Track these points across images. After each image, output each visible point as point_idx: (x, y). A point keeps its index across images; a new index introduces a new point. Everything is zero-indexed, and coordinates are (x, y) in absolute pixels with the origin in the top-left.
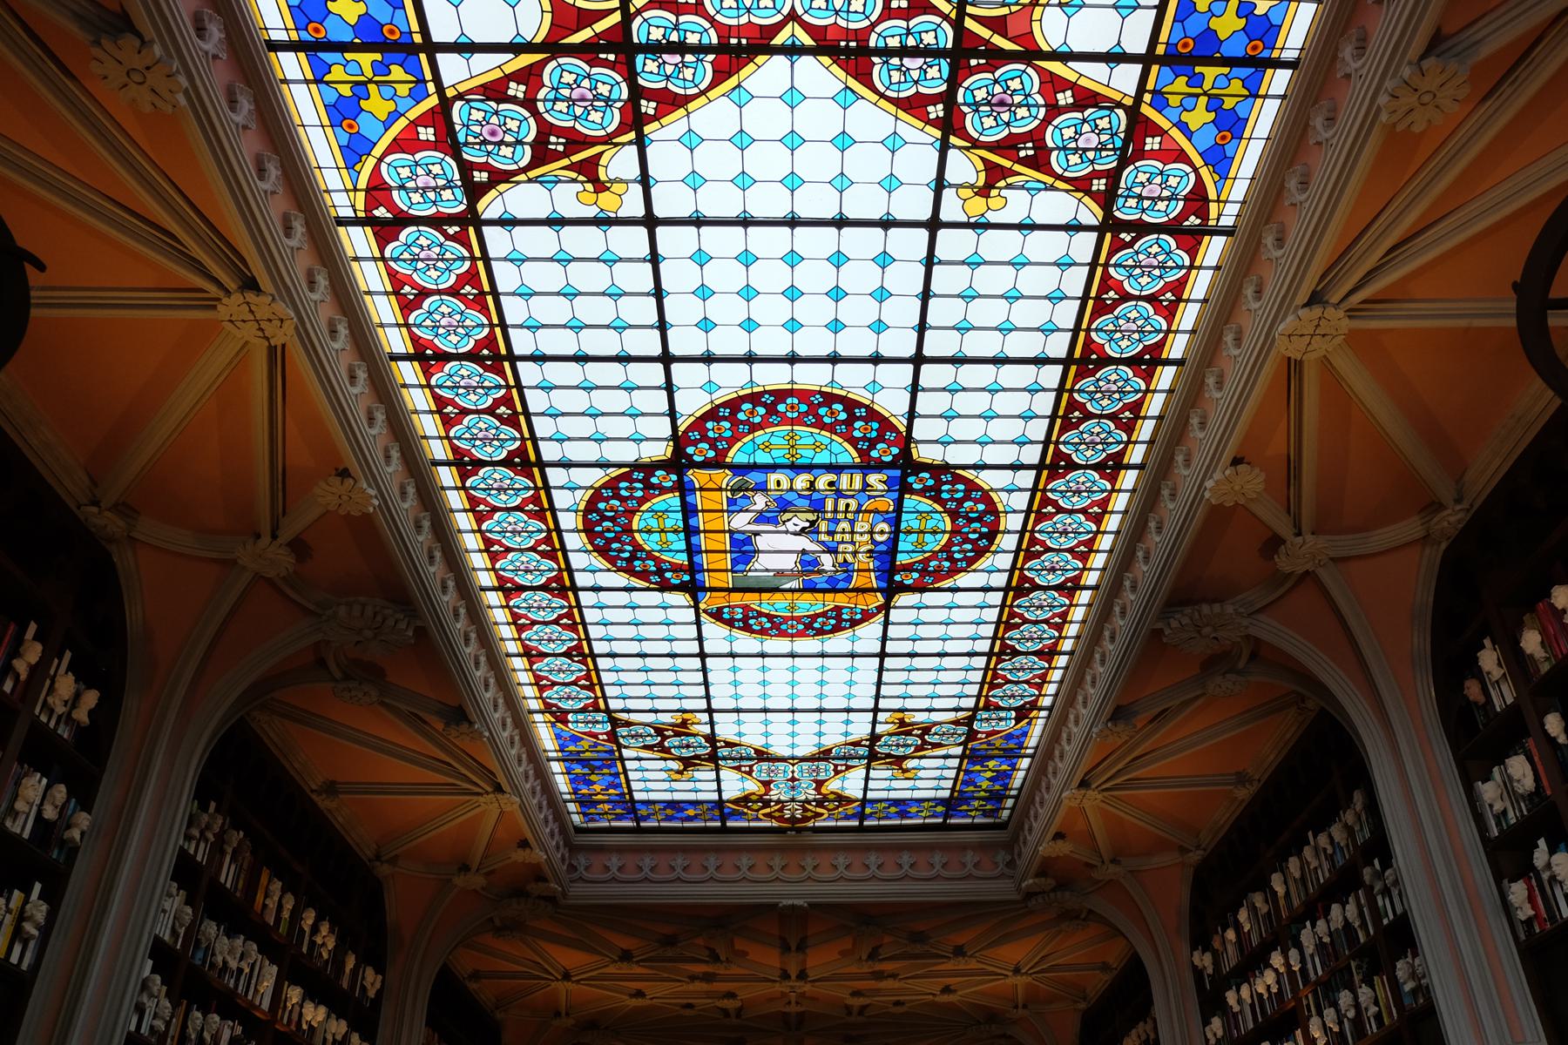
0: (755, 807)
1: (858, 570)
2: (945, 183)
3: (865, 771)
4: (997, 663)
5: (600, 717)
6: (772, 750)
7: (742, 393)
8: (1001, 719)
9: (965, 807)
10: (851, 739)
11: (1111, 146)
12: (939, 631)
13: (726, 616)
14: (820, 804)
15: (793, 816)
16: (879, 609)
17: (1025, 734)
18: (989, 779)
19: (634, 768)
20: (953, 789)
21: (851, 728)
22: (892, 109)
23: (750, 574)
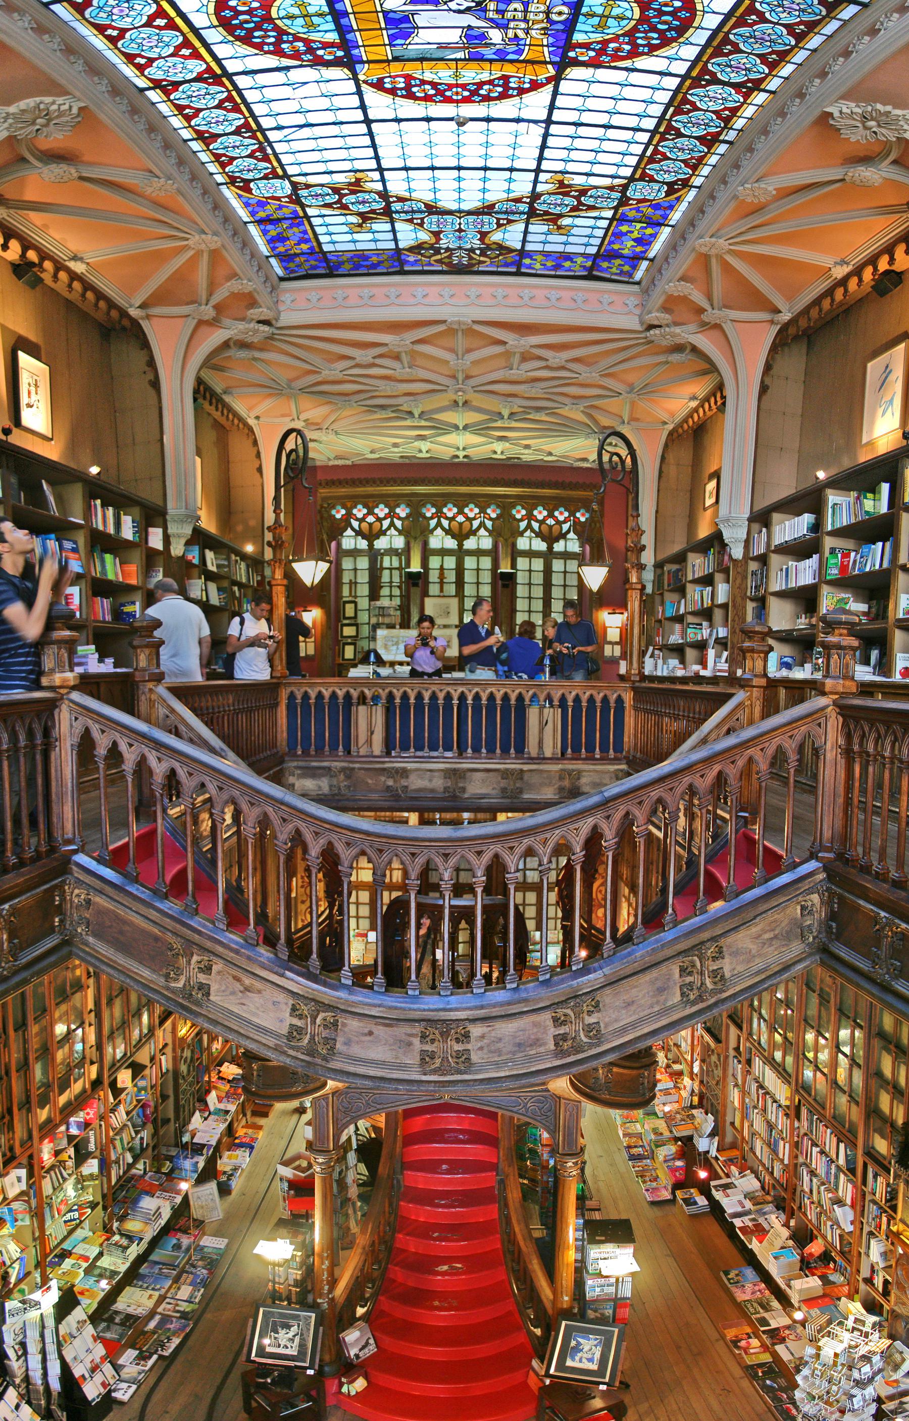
6: (440, 204)
10: (512, 196)
13: (388, 86)
14: (483, 254)
23: (410, 47)
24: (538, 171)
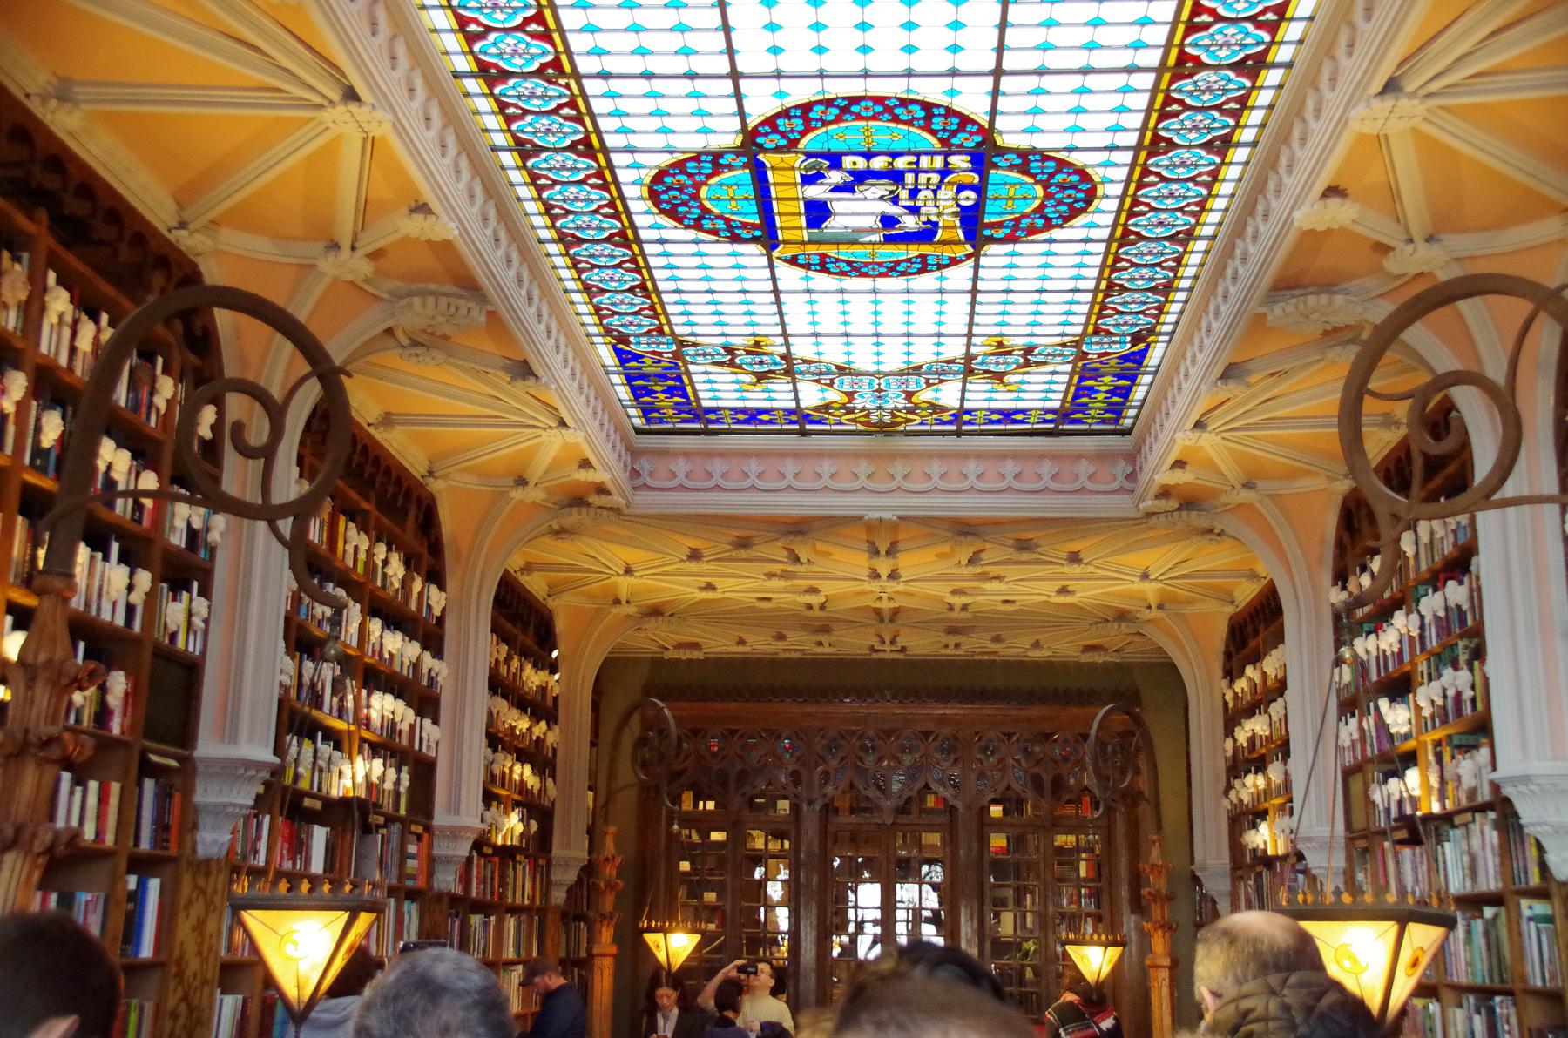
0: (837, 413)
1: (944, 228)
8: (1115, 343)
9: (1079, 416)
16: (968, 256)
18: (1107, 392)
20: (1064, 400)
21: (941, 349)
24: (970, 335)
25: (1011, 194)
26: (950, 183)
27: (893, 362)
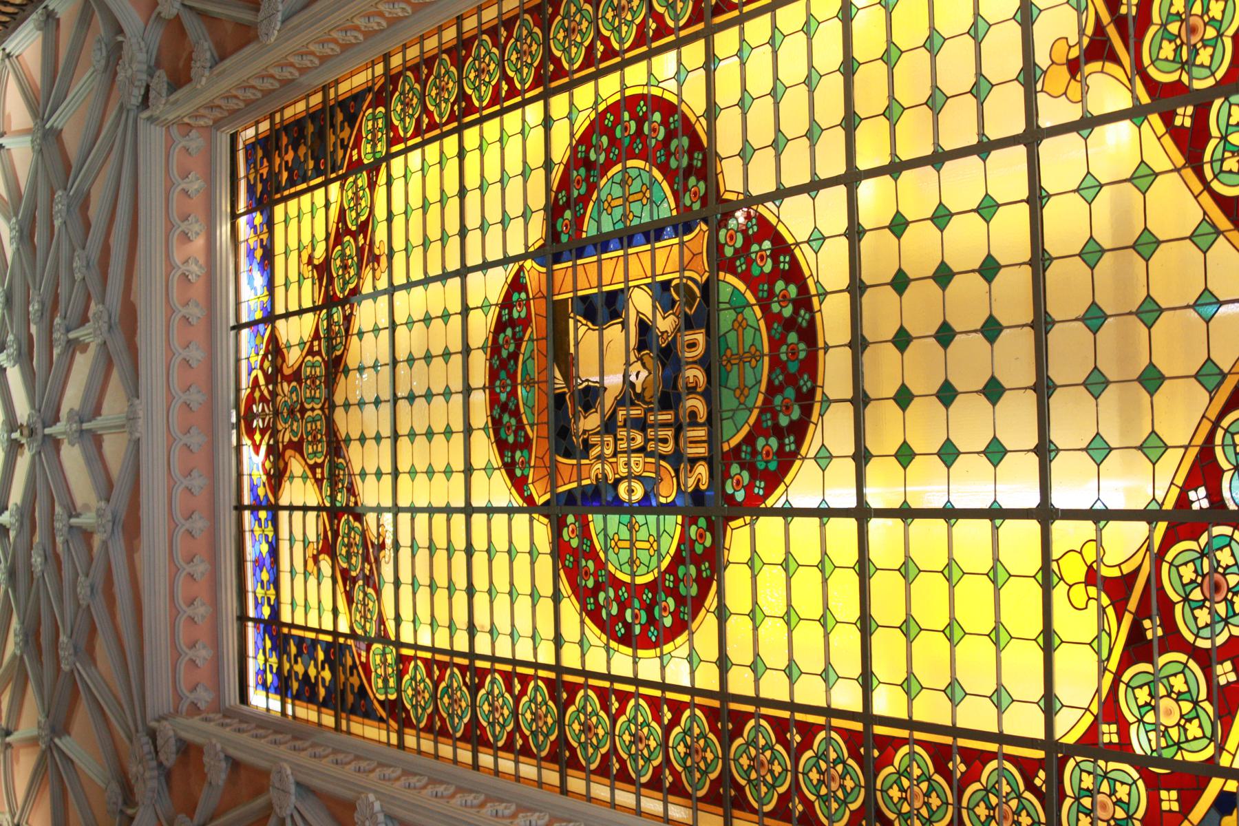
1: (579, 465)
2: (1102, 523)
3: (315, 504)
4: (459, 666)
5: (381, 148)
7: (810, 282)
8: (386, 681)
9: (269, 644)
11: (1163, 744)
12: (502, 584)
13: (515, 297)
15: (255, 416)
16: (529, 500)
17: (368, 714)
18: (306, 674)
19: (316, 201)
20: (292, 626)
21: (371, 479)
22: (1200, 440)
25: (638, 545)
26: (658, 467)
27: (346, 423)
